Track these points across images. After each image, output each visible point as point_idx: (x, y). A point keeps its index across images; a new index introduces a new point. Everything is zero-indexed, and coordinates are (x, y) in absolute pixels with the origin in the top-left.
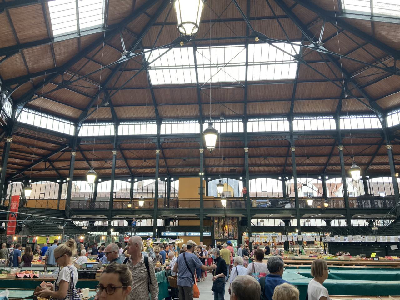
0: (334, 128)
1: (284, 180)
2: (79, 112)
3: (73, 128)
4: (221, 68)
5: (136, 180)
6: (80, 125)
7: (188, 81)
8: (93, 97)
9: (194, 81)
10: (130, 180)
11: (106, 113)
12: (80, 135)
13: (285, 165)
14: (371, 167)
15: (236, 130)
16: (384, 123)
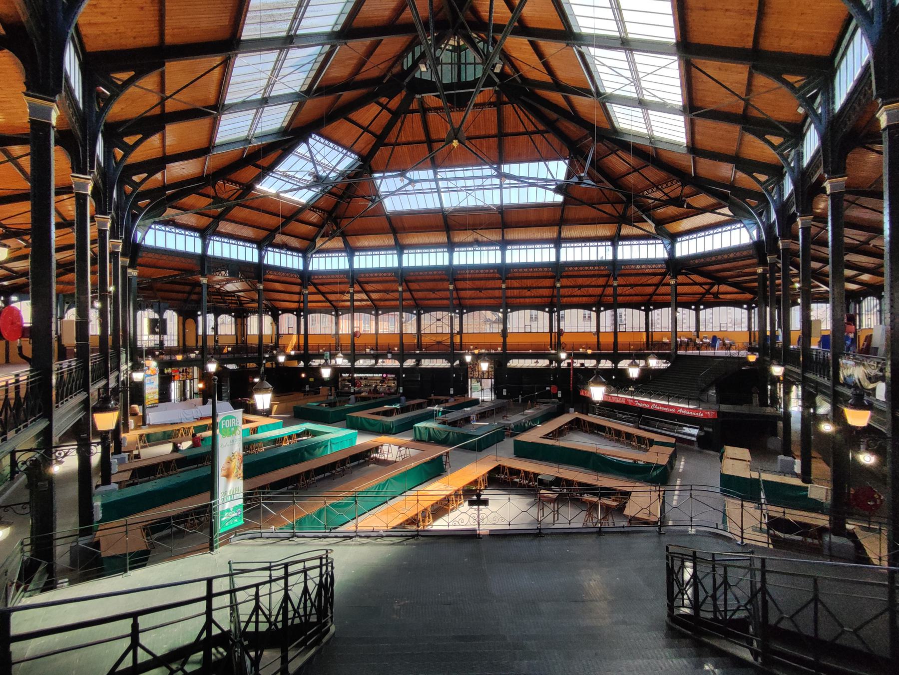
0: (610, 257)
1: (551, 313)
2: (306, 243)
3: (301, 259)
4: (470, 192)
5: (380, 312)
6: (309, 256)
7: (431, 206)
8: (319, 226)
9: (438, 206)
10: (373, 312)
11: (338, 243)
12: (310, 269)
13: (553, 296)
14: (655, 297)
15: (492, 261)
16: (672, 252)
